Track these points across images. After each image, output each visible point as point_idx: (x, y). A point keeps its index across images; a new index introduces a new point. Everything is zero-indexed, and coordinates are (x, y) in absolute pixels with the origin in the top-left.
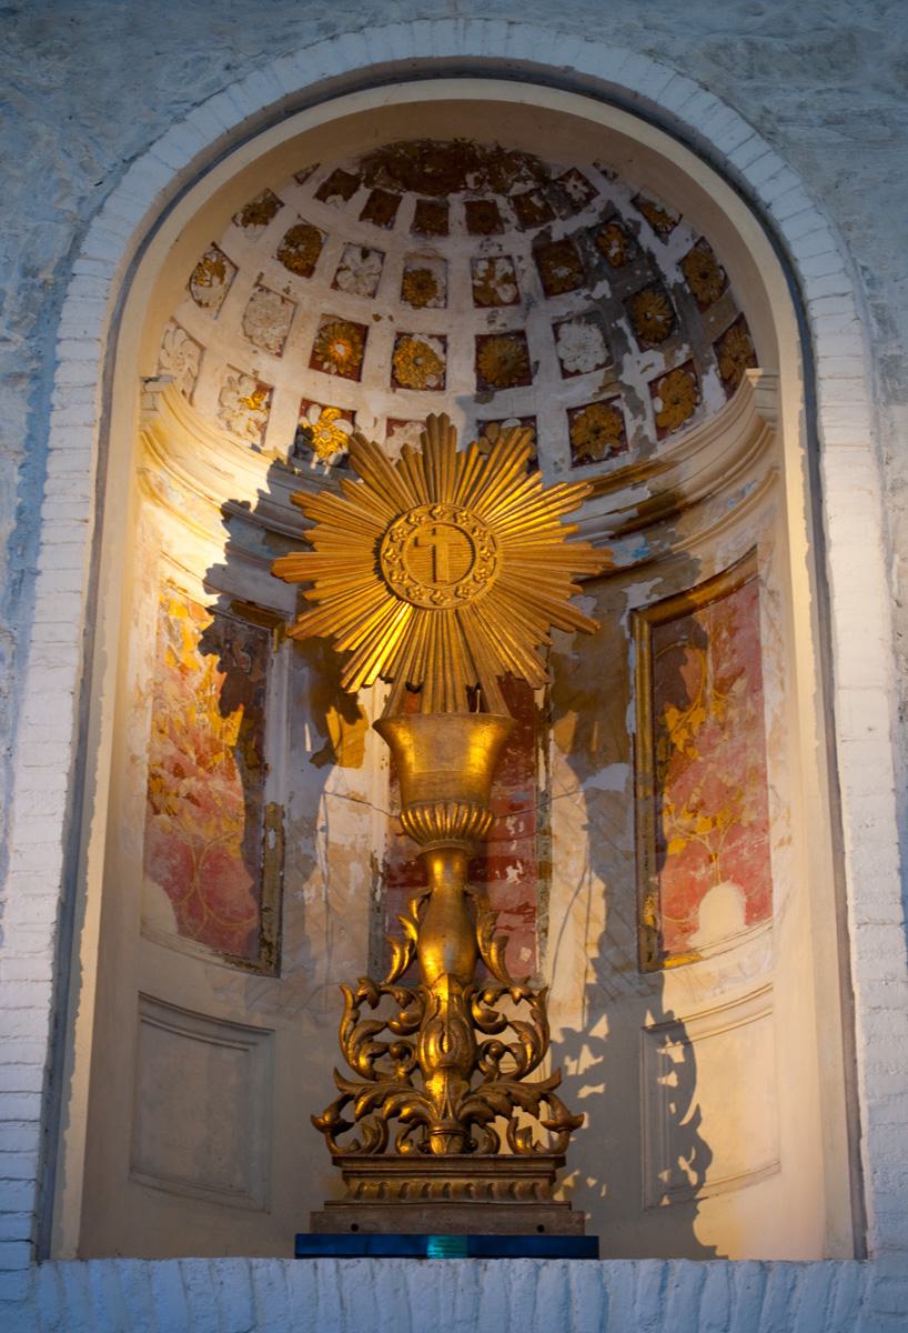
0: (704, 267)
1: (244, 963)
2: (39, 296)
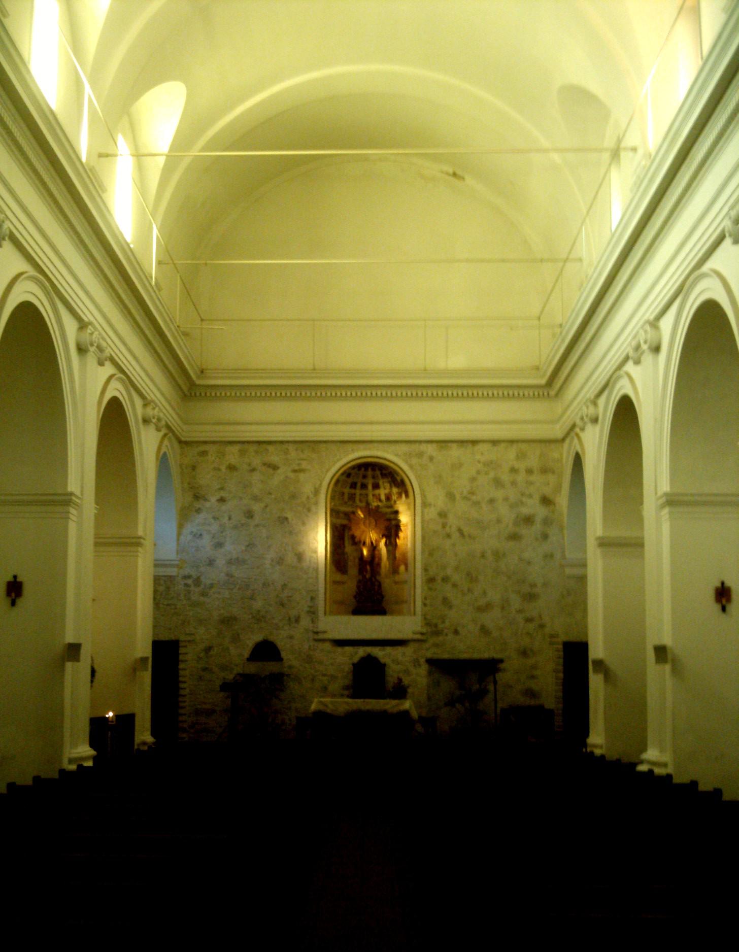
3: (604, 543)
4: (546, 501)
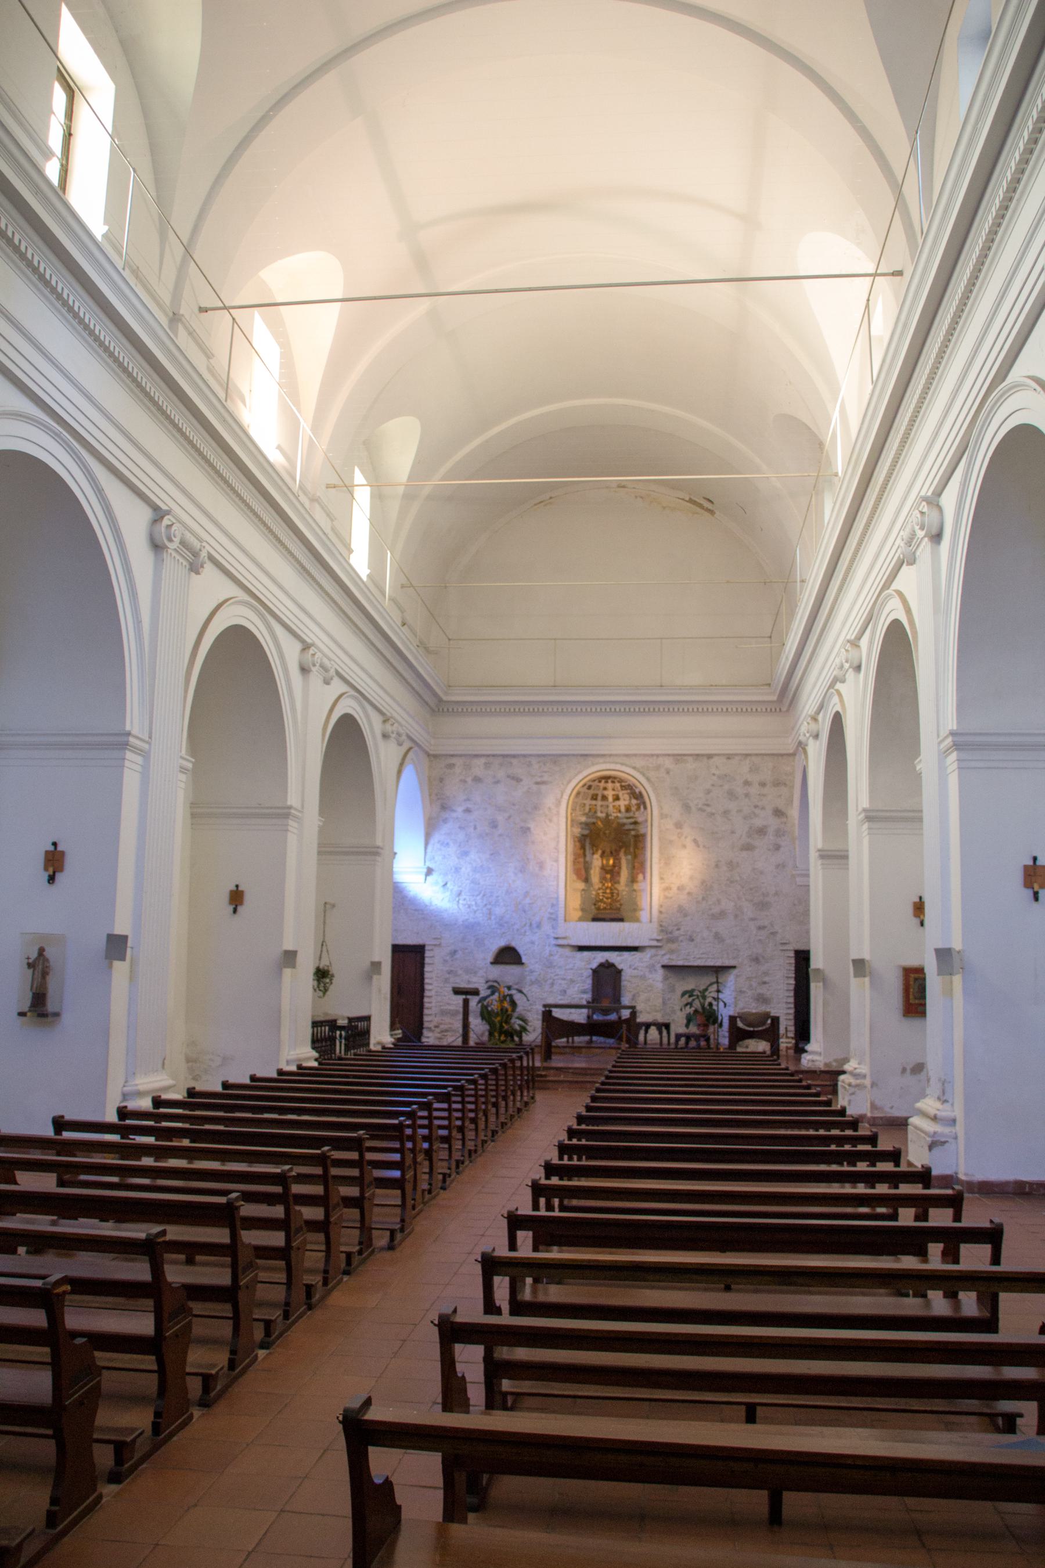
0: (640, 793)
3: (825, 855)
4: (778, 813)
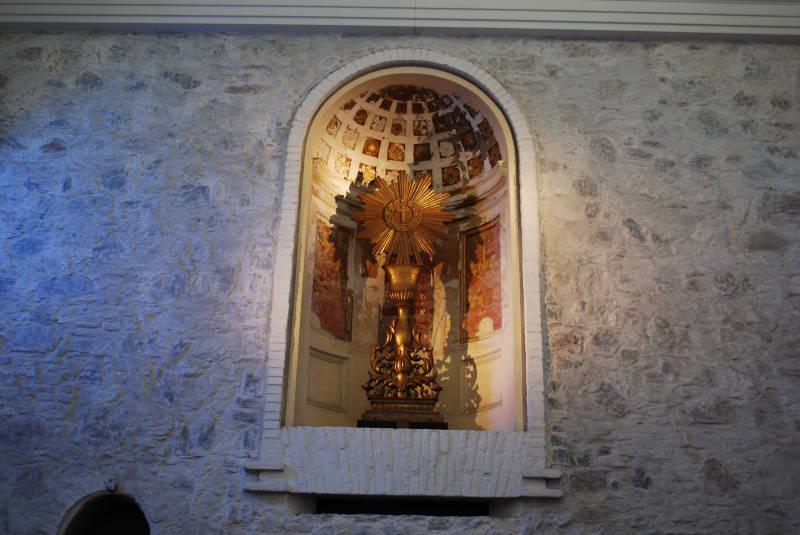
0: (486, 128)
1: (341, 338)
2: (281, 131)
